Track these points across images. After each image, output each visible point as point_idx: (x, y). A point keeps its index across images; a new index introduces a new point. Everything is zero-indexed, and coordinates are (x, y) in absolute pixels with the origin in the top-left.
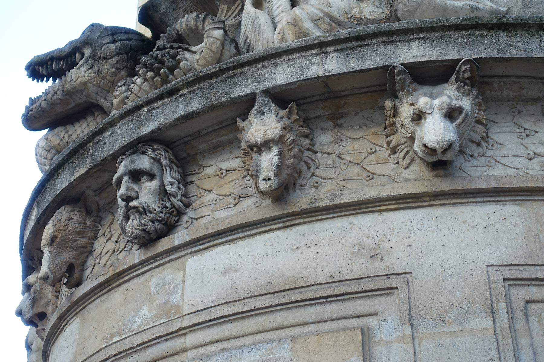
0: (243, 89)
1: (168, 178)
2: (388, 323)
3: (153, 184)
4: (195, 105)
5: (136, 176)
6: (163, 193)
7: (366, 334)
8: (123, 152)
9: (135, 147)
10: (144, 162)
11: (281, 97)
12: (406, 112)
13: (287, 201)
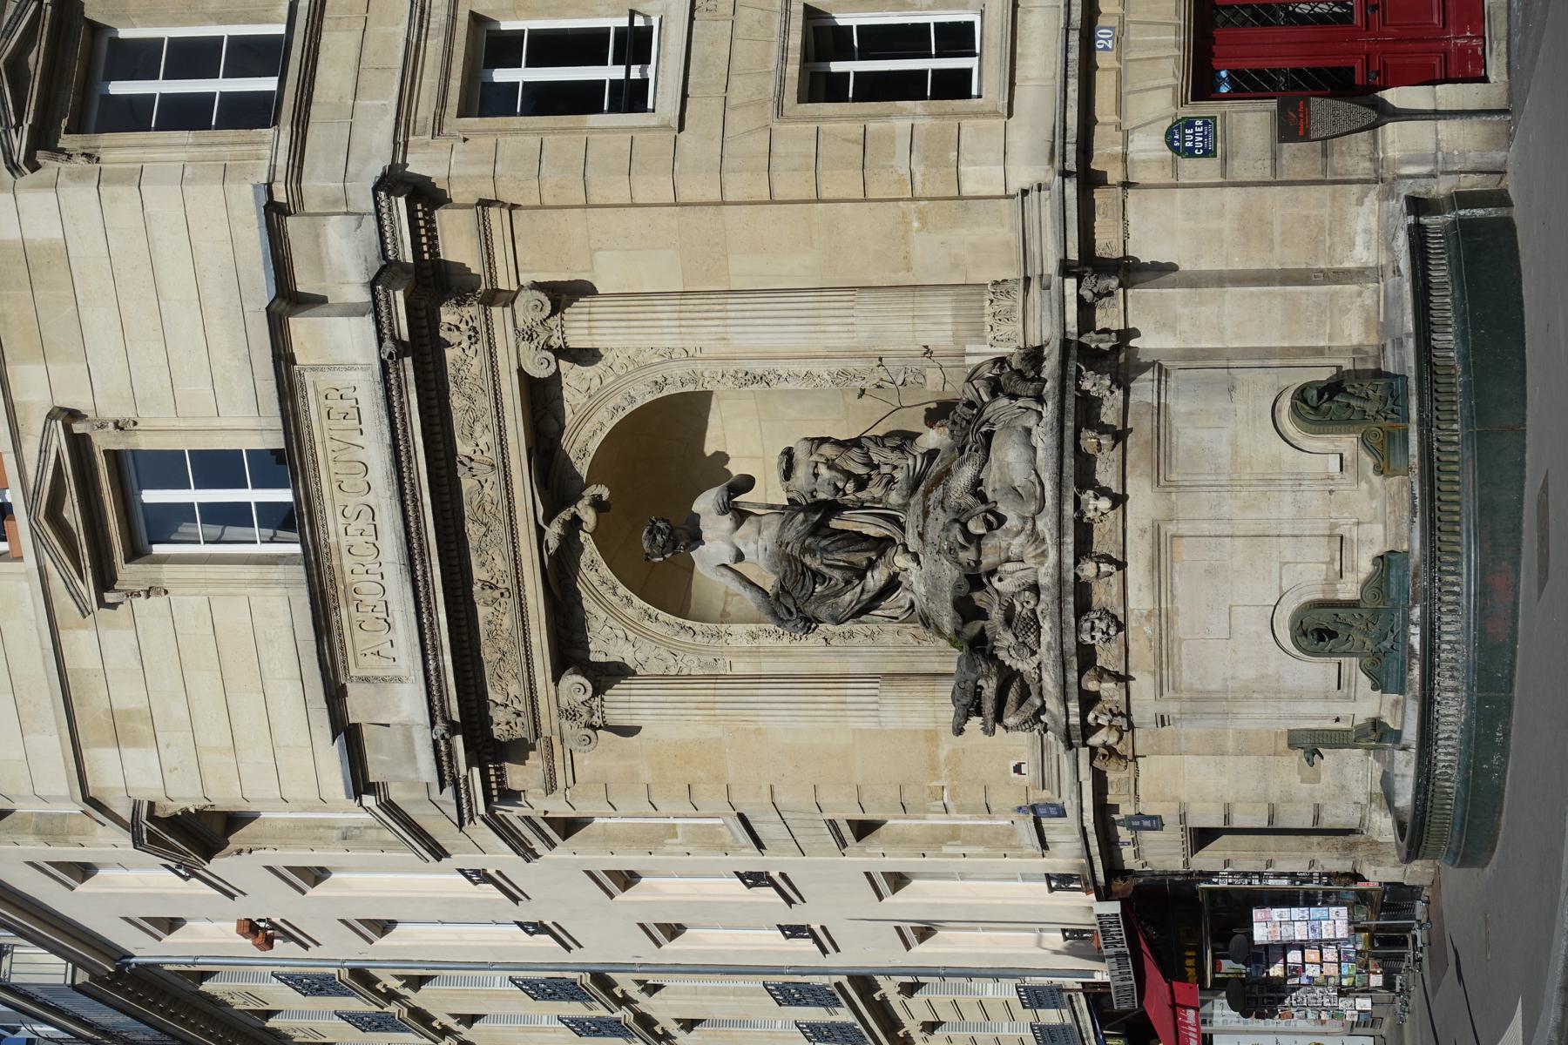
0: (1071, 577)
1: (1093, 616)
2: (1171, 528)
4: (1071, 599)
5: (1093, 629)
6: (1100, 619)
7: (1173, 536)
9: (1078, 630)
10: (1087, 625)
11: (1077, 562)
12: (1090, 514)
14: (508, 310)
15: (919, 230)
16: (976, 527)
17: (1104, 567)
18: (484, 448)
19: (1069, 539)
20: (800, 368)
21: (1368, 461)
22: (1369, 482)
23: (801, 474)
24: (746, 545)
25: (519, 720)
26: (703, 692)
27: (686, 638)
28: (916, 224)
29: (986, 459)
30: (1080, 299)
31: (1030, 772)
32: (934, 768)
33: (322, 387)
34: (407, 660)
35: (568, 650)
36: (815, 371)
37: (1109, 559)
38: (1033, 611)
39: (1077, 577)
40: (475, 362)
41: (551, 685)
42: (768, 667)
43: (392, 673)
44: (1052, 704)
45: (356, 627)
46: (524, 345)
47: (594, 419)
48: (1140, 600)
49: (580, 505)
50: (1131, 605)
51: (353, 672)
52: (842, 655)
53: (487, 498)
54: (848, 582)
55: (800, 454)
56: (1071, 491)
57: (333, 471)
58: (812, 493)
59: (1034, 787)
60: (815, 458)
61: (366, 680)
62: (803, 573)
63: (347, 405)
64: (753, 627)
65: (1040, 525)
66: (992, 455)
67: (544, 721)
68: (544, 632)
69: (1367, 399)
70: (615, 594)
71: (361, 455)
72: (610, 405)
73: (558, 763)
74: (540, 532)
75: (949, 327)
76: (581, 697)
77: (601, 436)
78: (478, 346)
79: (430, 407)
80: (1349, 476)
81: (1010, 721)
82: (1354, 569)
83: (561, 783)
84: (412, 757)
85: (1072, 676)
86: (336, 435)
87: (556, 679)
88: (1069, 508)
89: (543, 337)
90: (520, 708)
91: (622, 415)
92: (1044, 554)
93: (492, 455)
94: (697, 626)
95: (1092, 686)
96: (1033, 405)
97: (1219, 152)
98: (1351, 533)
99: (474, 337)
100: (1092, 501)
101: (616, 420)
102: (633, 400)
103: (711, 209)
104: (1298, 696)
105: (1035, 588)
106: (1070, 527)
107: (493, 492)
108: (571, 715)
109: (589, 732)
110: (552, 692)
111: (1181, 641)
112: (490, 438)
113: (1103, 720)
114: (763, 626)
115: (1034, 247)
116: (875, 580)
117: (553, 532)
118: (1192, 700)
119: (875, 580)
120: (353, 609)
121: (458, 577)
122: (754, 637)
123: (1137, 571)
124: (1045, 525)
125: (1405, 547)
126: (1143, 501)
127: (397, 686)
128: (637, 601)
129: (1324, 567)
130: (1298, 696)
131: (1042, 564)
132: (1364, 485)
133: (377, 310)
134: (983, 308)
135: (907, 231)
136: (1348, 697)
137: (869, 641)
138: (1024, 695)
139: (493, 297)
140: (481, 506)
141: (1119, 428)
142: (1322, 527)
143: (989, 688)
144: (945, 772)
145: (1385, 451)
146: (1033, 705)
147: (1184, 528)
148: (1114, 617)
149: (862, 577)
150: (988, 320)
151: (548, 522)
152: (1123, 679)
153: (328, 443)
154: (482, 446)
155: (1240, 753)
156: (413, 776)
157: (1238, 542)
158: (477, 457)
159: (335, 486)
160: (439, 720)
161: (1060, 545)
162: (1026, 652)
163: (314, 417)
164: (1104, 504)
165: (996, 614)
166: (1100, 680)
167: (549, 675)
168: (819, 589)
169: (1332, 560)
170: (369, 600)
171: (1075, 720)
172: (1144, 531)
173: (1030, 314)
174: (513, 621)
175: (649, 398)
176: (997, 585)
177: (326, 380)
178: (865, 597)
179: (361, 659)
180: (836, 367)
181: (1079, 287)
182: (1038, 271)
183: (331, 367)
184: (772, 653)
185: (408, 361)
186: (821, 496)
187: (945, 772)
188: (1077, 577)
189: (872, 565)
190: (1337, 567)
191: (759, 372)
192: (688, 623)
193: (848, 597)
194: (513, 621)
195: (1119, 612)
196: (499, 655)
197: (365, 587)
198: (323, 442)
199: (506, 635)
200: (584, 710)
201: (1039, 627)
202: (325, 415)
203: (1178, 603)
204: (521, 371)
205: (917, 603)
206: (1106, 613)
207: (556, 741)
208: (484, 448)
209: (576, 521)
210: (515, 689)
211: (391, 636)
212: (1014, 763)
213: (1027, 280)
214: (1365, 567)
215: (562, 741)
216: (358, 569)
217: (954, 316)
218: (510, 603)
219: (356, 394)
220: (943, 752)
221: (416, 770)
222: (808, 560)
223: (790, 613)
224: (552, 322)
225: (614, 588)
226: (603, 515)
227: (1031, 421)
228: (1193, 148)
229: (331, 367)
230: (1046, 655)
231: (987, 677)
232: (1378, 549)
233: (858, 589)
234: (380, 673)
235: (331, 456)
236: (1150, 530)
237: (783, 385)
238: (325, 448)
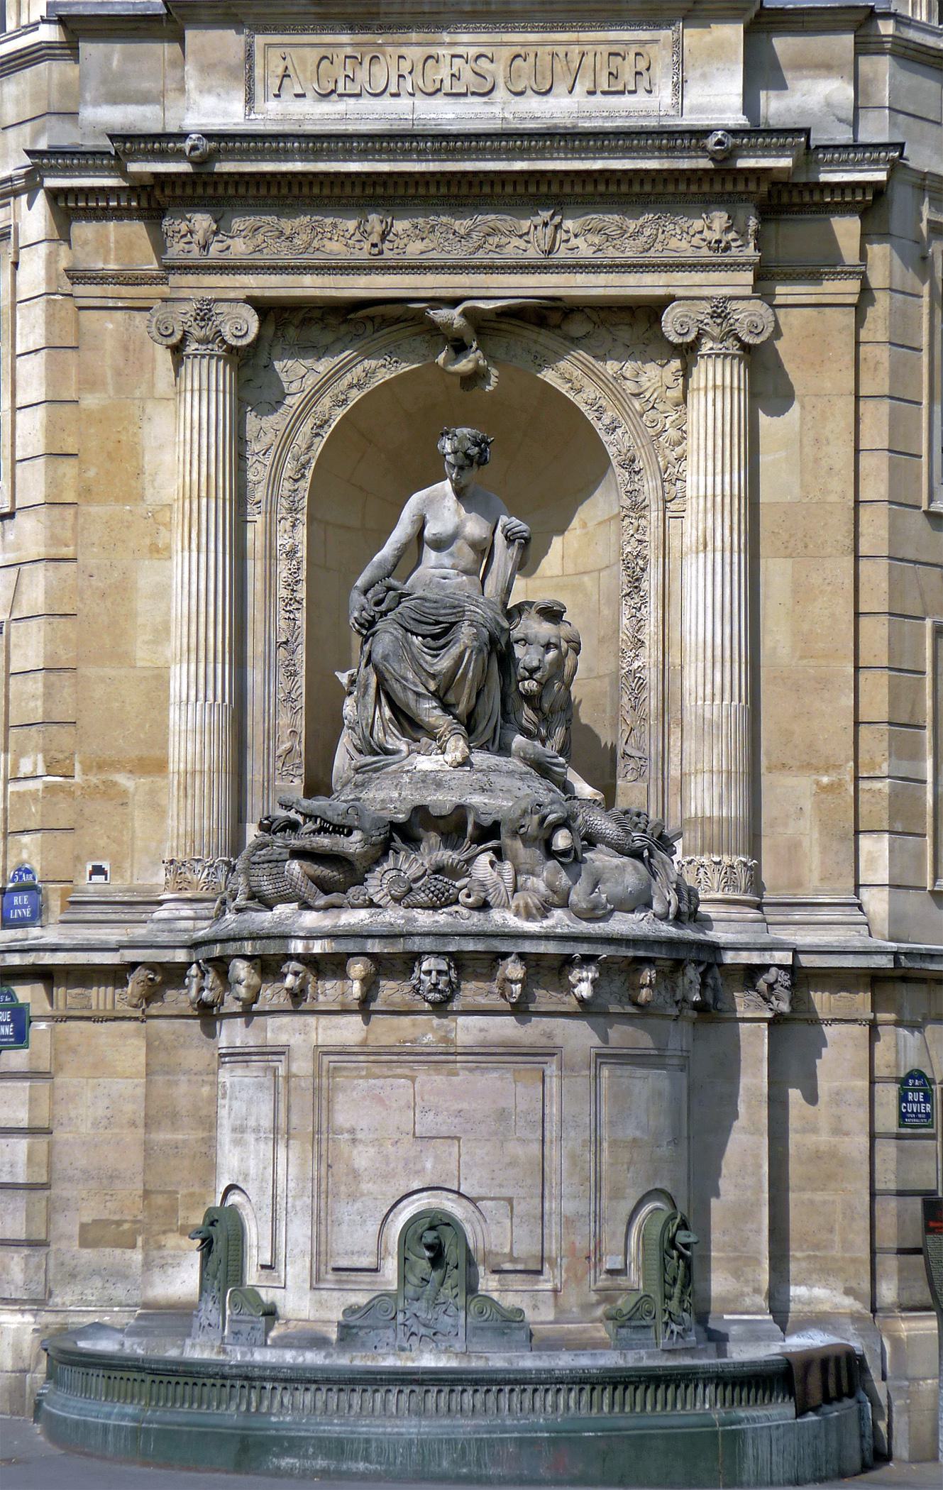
1: (453, 973)
2: (552, 1069)
3: (445, 978)
5: (439, 972)
6: (450, 983)
8: (429, 953)
9: (439, 954)
11: (522, 956)
13: (521, 1010)
14: (748, 291)
15: (818, 783)
16: (562, 840)
17: (517, 988)
18: (570, 245)
19: (550, 948)
20: (651, 630)
21: (624, 1303)
22: (599, 1303)
23: (545, 630)
24: (451, 555)
25: (195, 248)
26: (225, 484)
27: (289, 468)
28: (825, 780)
29: (622, 851)
30: (765, 968)
31: (91, 886)
32: (101, 767)
33: (653, 50)
34: (275, 113)
35: (288, 322)
36: (644, 652)
37: (526, 996)
38: (457, 902)
39: (505, 956)
40: (684, 244)
41: (242, 294)
42: (255, 569)
43: (259, 90)
44: (310, 919)
45: (323, 51)
46: (706, 307)
47: (586, 381)
48: (467, 1029)
49: (479, 353)
50: (462, 1020)
51: (260, 40)
52: (267, 657)
53: (504, 240)
54: (434, 676)
55: (564, 630)
56: (604, 952)
57: (540, 50)
58: (525, 641)
59: (65, 893)
60: (564, 645)
61: (249, 56)
62: (438, 623)
63: (627, 76)
64: (303, 552)
65: (558, 913)
66: (625, 859)
67: (190, 279)
68: (318, 293)
69: (681, 1301)
70: (351, 386)
71: (560, 88)
72: (603, 402)
73: (110, 290)
74: (454, 302)
75: (716, 814)
76: (227, 331)
77: (563, 388)
78: (705, 251)
79: (631, 183)
80: (603, 1281)
81: (295, 866)
83: (80, 290)
84: (115, 99)
85: (374, 947)
86: (589, 60)
87: (251, 301)
88: (584, 949)
89: (716, 331)
90: (214, 248)
91: (591, 416)
92: (529, 917)
93: (562, 253)
94: (305, 484)
95: (357, 968)
96: (672, 909)
97: (904, 1131)
98: (545, 1284)
99: (717, 246)
100: (590, 975)
101: (583, 408)
102: (612, 429)
103: (849, 542)
105: (484, 906)
106: (566, 949)
107: (514, 248)
108: (204, 315)
109: (178, 336)
110: (232, 295)
111: (413, 1079)
112: (586, 256)
113: (290, 981)
114: (304, 565)
115: (798, 915)
116: (429, 712)
117: (453, 316)
118: (317, 1090)
119: (429, 712)
120: (349, 51)
121: (401, 191)
122: (291, 553)
123: (505, 1028)
124: (559, 920)
126: (579, 1036)
127: (241, 95)
128: (340, 413)
129: (507, 1250)
130: (321, 1220)
131: (517, 914)
132: (594, 1297)
133: (756, 133)
134: (738, 854)
135: (817, 769)
136: (318, 1280)
137: (281, 696)
138: (325, 887)
139: (765, 276)
140: (494, 232)
141: (532, 1007)
142: (552, 1248)
143: (353, 844)
144: (94, 779)
145: (630, 1322)
146: (314, 896)
147: (553, 1084)
148: (449, 999)
149: (435, 695)
150: (726, 859)
151: (464, 314)
152: (365, 1007)
153: (577, 49)
154: (574, 242)
155: (148, 1149)
156: (88, 96)
157: (536, 1147)
158: (561, 235)
159: (517, 50)
160: (213, 145)
161: (547, 937)
162: (397, 891)
163: (612, 35)
164: (584, 989)
165: (447, 856)
166: (363, 980)
167: (257, 293)
168: (417, 641)
169: (514, 1260)
170: (362, 75)
171: (297, 947)
172: (550, 1037)
173: (734, 909)
174: (334, 257)
175: (611, 450)
176: (485, 859)
177: (662, 58)
178: (411, 696)
179: (279, 51)
180: (652, 676)
181: (780, 967)
182: (770, 919)
183: (680, 64)
184: (270, 576)
185: (705, 163)
186: (519, 651)
187: (94, 779)
188: (505, 956)
189: (447, 708)
190: (507, 1266)
191: (644, 585)
192: (309, 474)
193: (410, 675)
194: (334, 257)
195: (455, 1005)
196: (288, 232)
197: (380, 72)
198: (578, 43)
199: (316, 244)
200: (208, 331)
201: (434, 908)
202: (615, 49)
203: (463, 1075)
204: (672, 299)
205: (396, 758)
206: (454, 988)
207: (163, 290)
208: (570, 245)
209: (460, 348)
210: (239, 248)
211: (310, 94)
212: (106, 866)
213: (759, 906)
214: (510, 1301)
215: (165, 300)
216: (405, 66)
217: (729, 819)
218: (363, 252)
219: (641, 92)
220: (123, 780)
221: (96, 103)
222: (465, 634)
223: (378, 603)
224: (732, 346)
225: (359, 386)
226: (458, 381)
227: (657, 907)
228: (907, 1101)
229: (680, 64)
230: (393, 916)
231: (364, 841)
232: (529, 1315)
233: (422, 690)
234: (258, 72)
235: (561, 50)
236: (550, 1043)
237: (626, 612)
238: (569, 43)
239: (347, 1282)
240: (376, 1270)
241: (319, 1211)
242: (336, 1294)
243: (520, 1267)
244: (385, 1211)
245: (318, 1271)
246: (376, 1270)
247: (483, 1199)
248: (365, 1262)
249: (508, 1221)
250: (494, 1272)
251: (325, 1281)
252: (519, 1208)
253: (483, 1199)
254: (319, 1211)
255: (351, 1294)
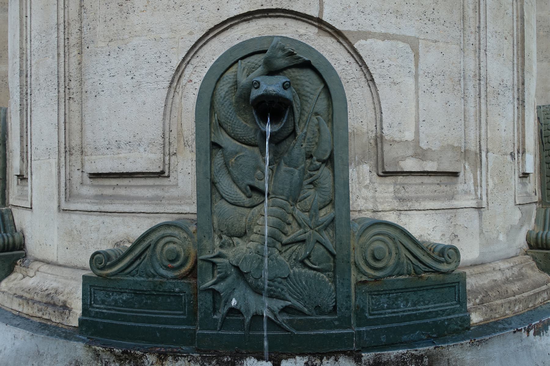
82: (404, 203)
104: (71, 91)
125: (476, 318)
129: (409, 135)
169: (421, 154)
190: (410, 165)
214: (424, 227)
239: (113, 198)
240: (160, 174)
241: (68, 79)
242: (93, 220)
243: (430, 166)
244: (176, 63)
245: (69, 180)
246: (160, 174)
247: (366, 35)
248: (144, 160)
249: (412, 81)
250: (387, 174)
251: (80, 196)
252: (430, 59)
253: (366, 35)
254: (68, 79)
255: (118, 219)
